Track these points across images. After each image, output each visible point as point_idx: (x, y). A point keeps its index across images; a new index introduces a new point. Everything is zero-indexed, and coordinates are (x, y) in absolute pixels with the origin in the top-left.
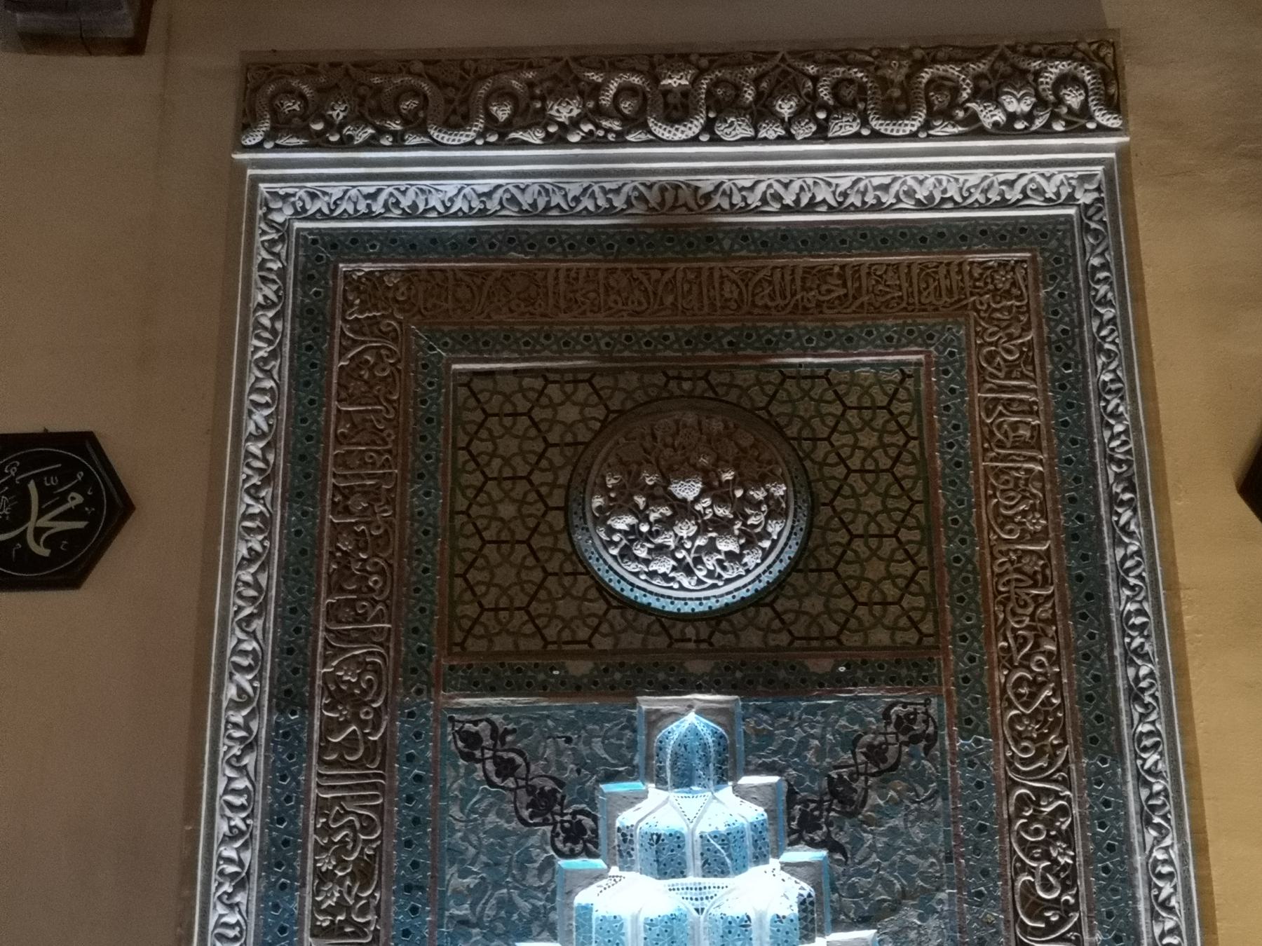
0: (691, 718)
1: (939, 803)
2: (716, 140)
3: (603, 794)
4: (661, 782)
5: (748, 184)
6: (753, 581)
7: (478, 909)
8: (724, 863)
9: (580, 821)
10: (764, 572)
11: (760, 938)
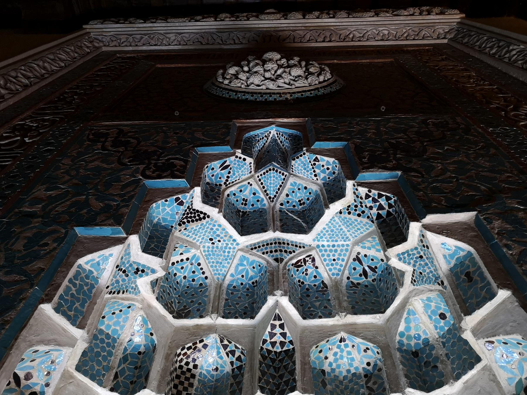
0: (273, 131)
1: (492, 151)
2: (286, 19)
3: (197, 153)
4: (247, 152)
5: (301, 33)
6: (314, 90)
7: (50, 207)
8: (301, 226)
9: (173, 162)
10: (321, 88)
11: (338, 298)
